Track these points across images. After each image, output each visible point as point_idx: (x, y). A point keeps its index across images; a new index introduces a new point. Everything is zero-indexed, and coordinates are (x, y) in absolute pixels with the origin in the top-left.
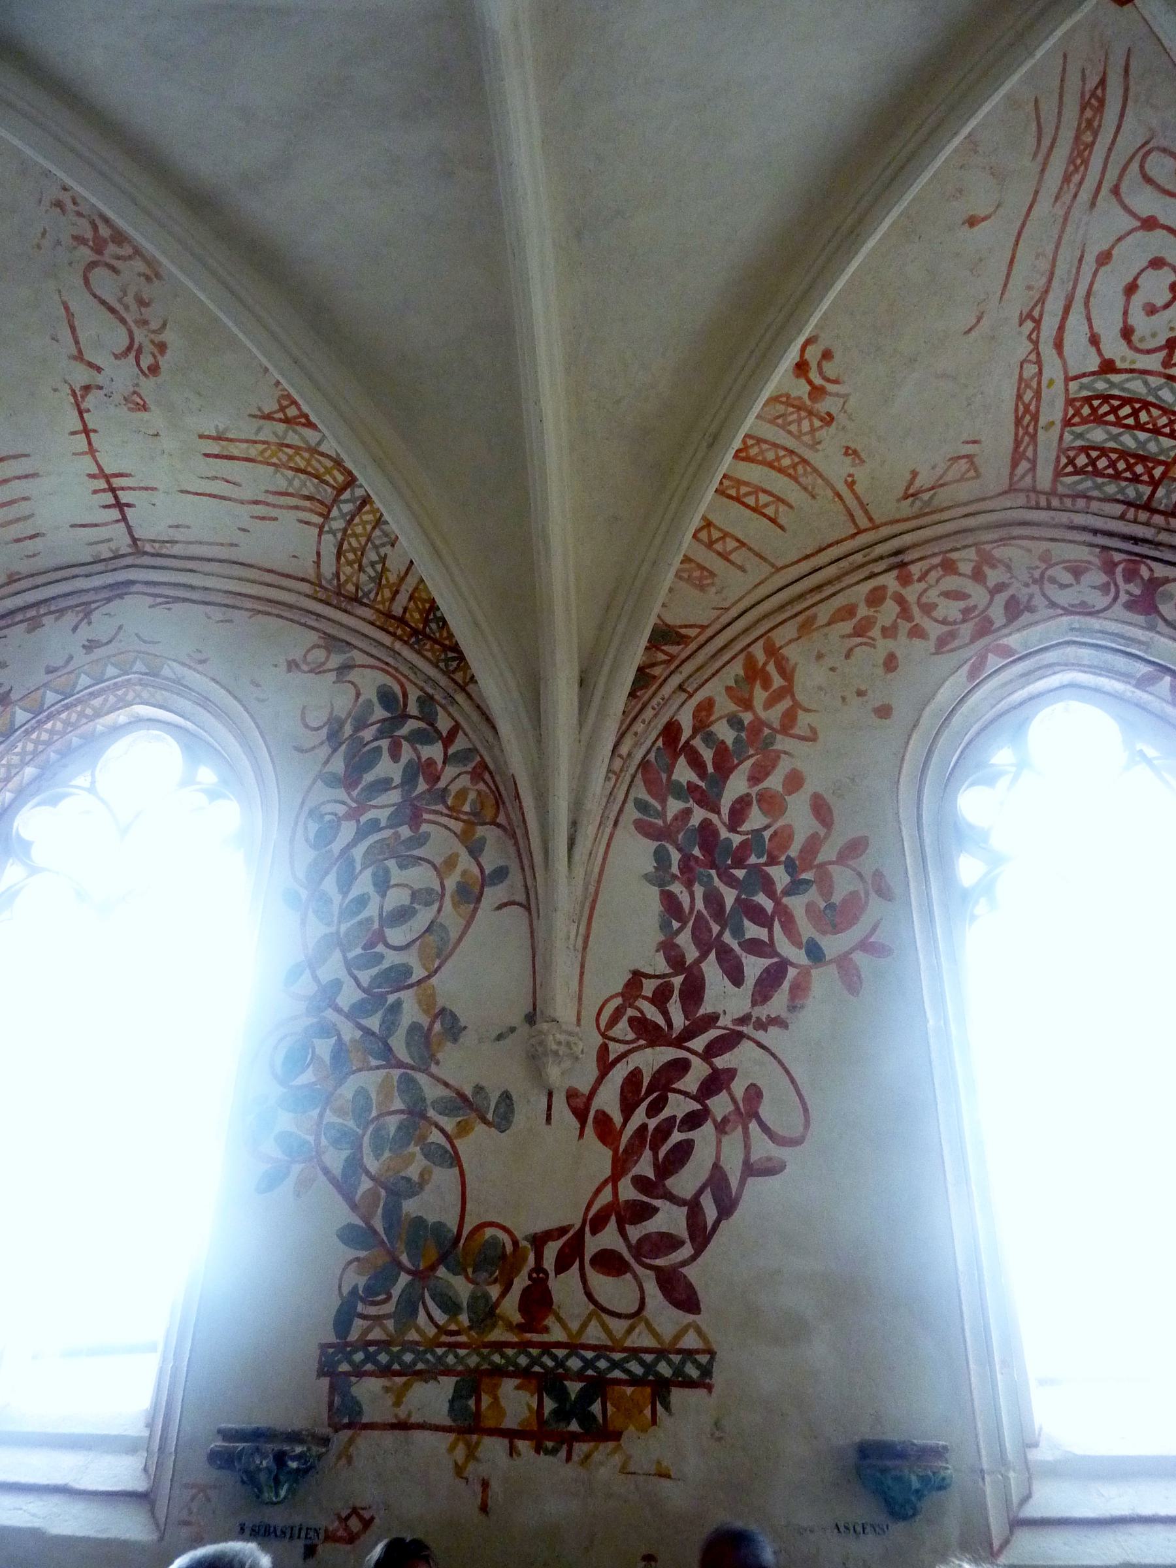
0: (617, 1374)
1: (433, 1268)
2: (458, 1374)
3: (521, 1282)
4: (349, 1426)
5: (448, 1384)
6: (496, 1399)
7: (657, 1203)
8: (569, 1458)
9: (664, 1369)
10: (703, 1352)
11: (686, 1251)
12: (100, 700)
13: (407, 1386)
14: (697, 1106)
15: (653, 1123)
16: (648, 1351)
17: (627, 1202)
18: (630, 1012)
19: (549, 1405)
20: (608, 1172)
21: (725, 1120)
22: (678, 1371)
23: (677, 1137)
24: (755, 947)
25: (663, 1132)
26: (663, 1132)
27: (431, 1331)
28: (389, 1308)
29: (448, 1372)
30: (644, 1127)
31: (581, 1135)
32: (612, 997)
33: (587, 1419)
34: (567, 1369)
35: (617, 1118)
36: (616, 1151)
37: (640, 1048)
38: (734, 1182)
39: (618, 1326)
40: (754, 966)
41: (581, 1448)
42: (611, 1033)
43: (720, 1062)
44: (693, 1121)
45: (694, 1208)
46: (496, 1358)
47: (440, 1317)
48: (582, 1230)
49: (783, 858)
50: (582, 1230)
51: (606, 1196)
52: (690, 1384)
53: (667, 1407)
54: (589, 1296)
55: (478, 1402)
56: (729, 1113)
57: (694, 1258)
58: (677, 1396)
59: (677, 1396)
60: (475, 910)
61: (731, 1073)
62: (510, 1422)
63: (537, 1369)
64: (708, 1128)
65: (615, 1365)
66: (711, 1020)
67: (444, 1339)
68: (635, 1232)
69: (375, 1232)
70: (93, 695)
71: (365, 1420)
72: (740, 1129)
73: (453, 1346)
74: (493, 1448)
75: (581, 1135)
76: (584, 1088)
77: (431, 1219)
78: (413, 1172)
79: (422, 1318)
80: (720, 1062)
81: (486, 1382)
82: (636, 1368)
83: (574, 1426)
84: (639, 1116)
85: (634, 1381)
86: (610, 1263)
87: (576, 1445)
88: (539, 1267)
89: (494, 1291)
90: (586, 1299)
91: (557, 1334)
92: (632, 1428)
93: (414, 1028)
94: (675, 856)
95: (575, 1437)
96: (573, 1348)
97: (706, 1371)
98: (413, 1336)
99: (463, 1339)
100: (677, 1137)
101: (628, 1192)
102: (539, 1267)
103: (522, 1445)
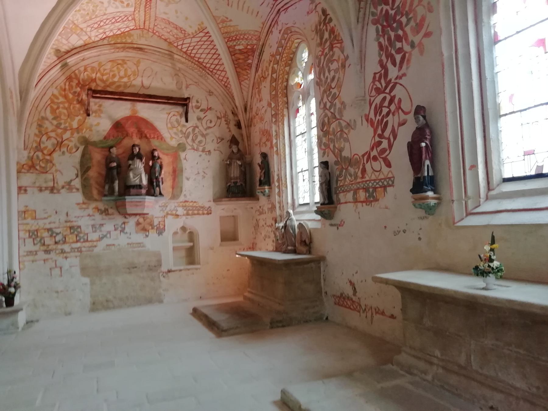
0: (378, 186)
1: (348, 167)
2: (353, 190)
3: (361, 167)
4: (339, 203)
5: (352, 192)
6: (359, 195)
7: (382, 140)
8: (371, 206)
9: (385, 183)
10: (392, 177)
11: (388, 152)
12: (288, 44)
13: (346, 194)
14: (388, 110)
15: (380, 118)
16: (382, 179)
17: (377, 142)
18: (375, 87)
19: (367, 195)
20: (373, 135)
21: (394, 112)
22: (388, 183)
23: (385, 120)
24: (399, 51)
25: (382, 120)
26: (382, 120)
27: (349, 182)
28: (343, 178)
29: (352, 190)
30: (379, 119)
31: (368, 126)
32: (371, 84)
33: (374, 197)
34: (370, 186)
35: (374, 119)
36: (374, 129)
37: (377, 97)
38: (396, 129)
39: (377, 174)
40: (398, 57)
41: (373, 203)
42: (371, 95)
43: (392, 94)
44: (388, 114)
45: (389, 139)
46: (358, 186)
47: (350, 178)
48: (370, 151)
49: (405, 13)
50: (370, 151)
51: (373, 142)
52: (390, 186)
53: (386, 192)
54: (372, 168)
55: (357, 196)
56: (395, 109)
57: (390, 153)
58: (388, 189)
59: (388, 189)
60: (345, 69)
61: (394, 96)
62: (362, 199)
63: (365, 187)
64: (391, 115)
65: (377, 184)
66: (390, 80)
67: (351, 183)
68: (379, 149)
69: (339, 161)
70: (287, 44)
71: (341, 202)
72: (397, 113)
73: (352, 184)
74: (359, 205)
75: (368, 126)
76: (367, 113)
77: (346, 156)
78: (342, 146)
79: (347, 179)
80: (392, 94)
81: (357, 191)
82: (381, 184)
83: (372, 199)
84: (378, 117)
85: (381, 187)
86: (375, 159)
87: (372, 203)
88: (364, 163)
89: (357, 170)
90: (371, 169)
91: (367, 178)
92: (381, 198)
93: (339, 108)
94: (380, 27)
95: (372, 201)
96: (370, 181)
97: (393, 182)
98: (346, 183)
99: (353, 182)
100: (385, 120)
101: (377, 139)
102: (364, 163)
103: (364, 204)
